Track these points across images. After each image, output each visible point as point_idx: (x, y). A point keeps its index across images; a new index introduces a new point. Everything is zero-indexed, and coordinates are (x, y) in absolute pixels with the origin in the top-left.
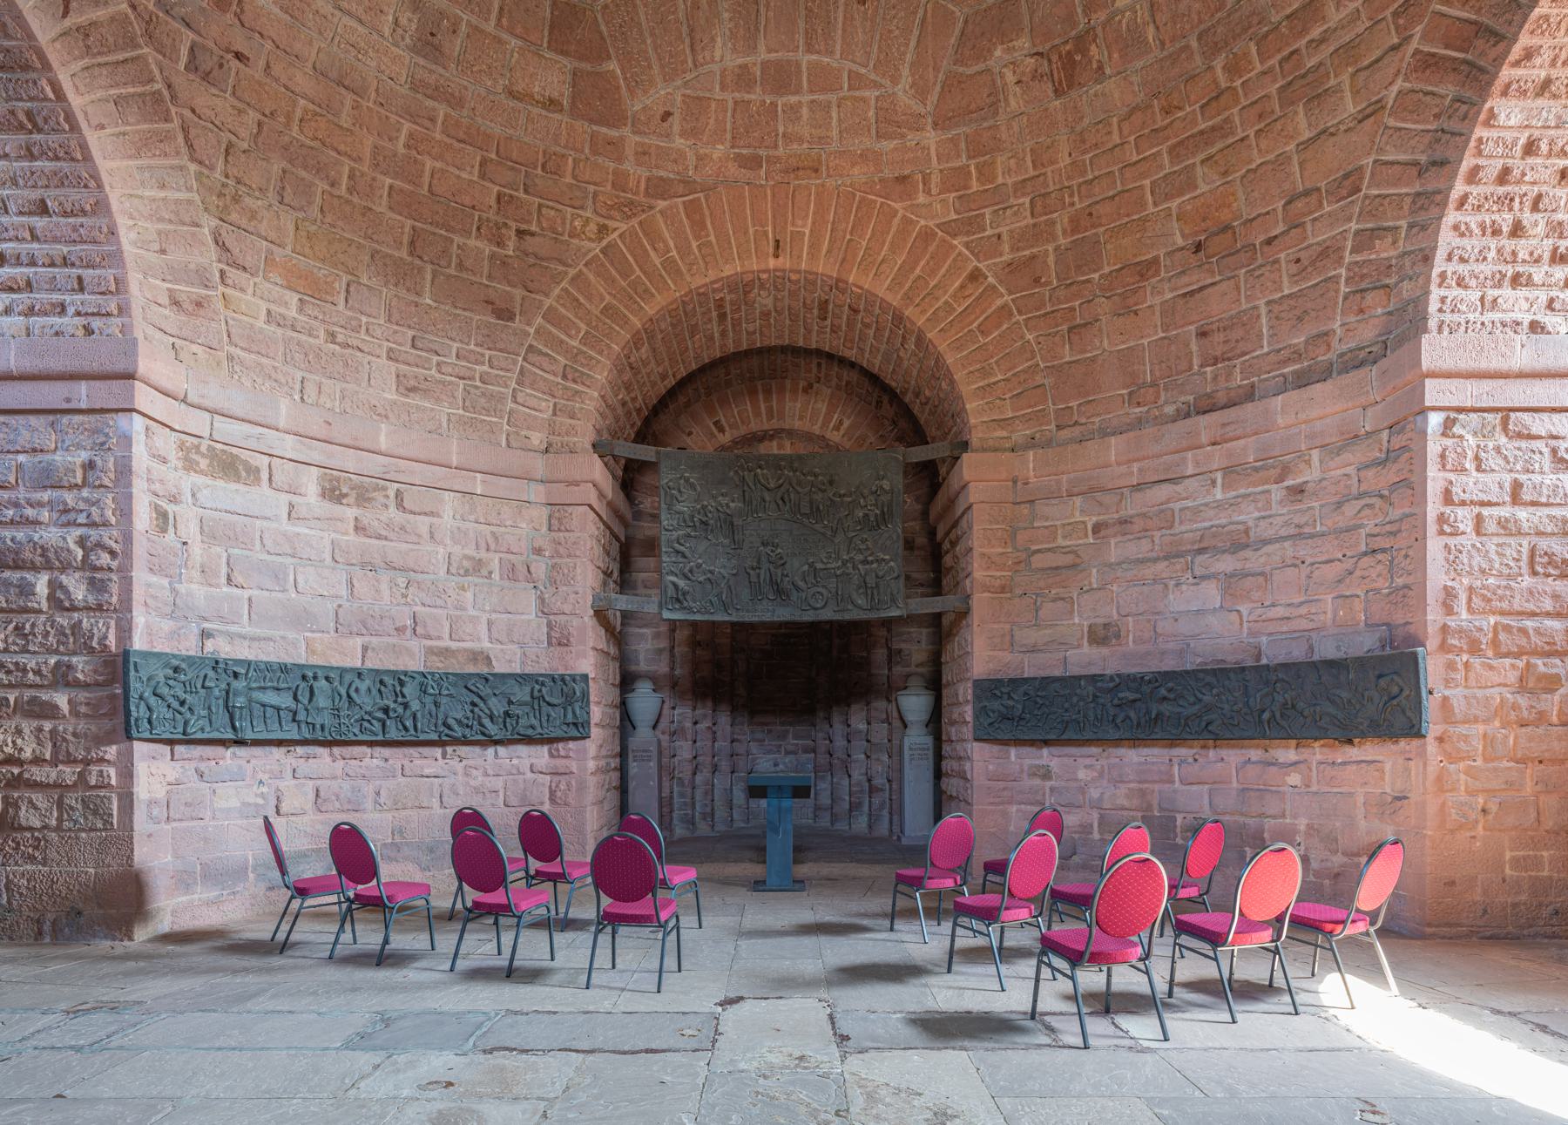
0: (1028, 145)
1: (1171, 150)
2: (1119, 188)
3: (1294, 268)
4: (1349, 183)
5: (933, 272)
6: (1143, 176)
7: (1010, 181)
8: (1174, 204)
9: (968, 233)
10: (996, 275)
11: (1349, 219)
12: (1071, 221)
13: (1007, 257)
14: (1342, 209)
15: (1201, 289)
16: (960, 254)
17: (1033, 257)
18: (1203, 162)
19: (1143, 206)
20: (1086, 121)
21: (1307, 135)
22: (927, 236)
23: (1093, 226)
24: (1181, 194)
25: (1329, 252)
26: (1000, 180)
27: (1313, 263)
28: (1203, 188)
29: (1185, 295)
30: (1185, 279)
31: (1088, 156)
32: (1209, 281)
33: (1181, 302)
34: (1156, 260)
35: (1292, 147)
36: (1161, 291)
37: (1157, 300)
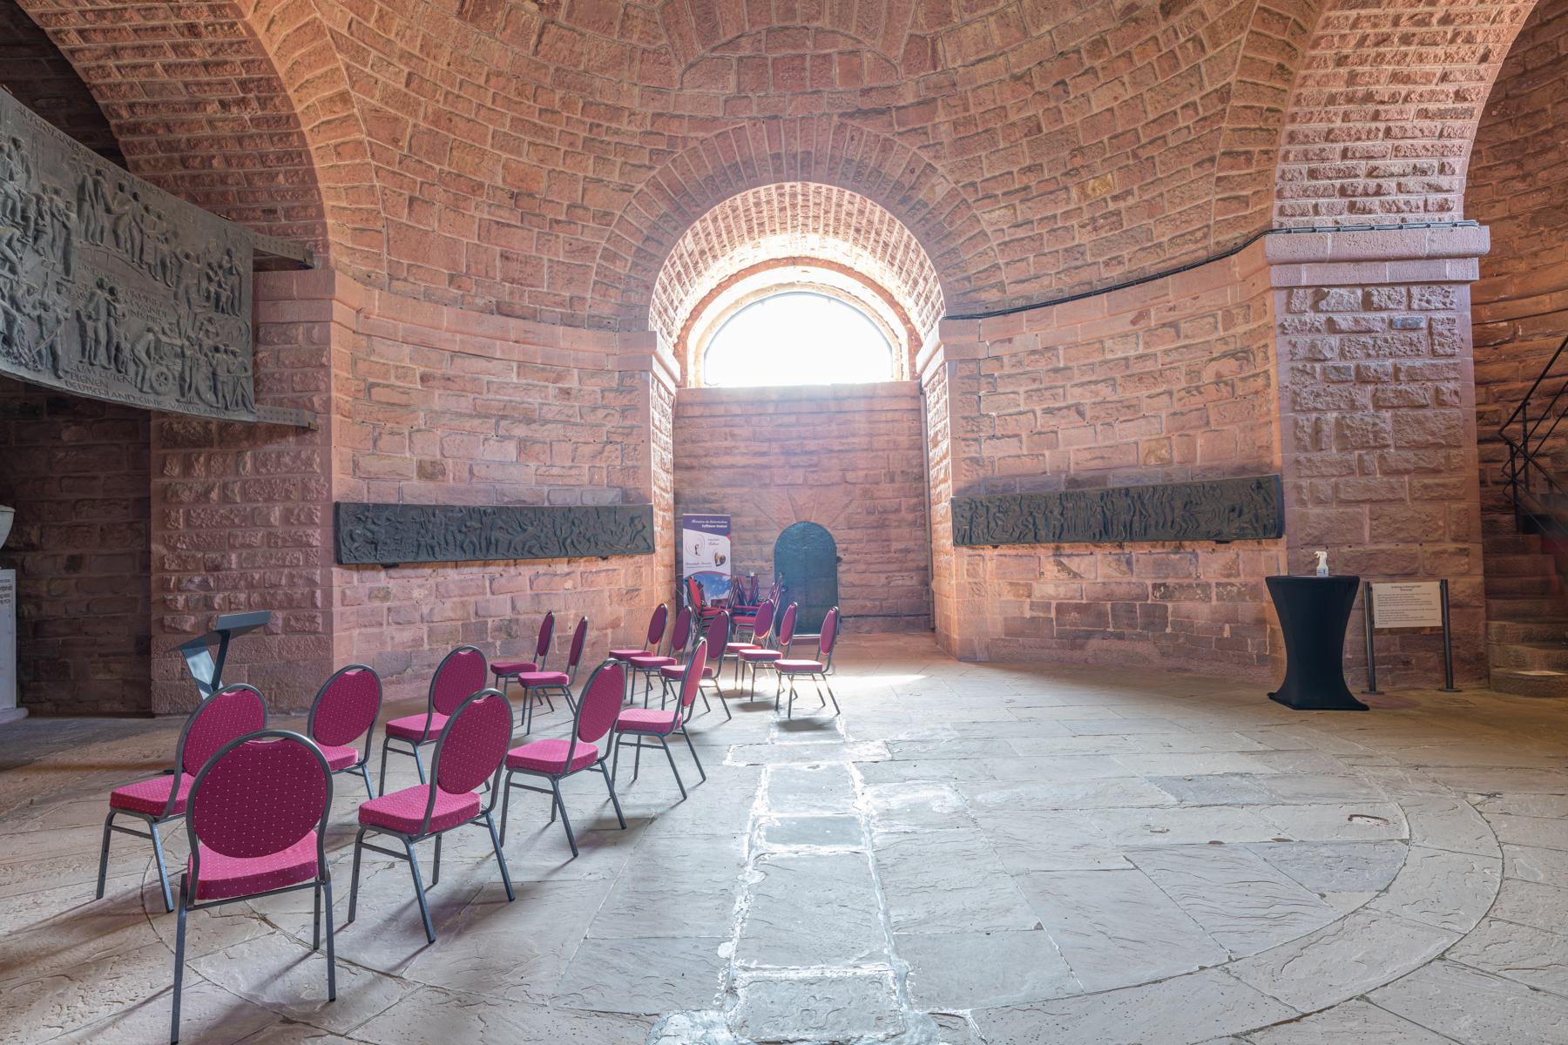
0: (423, 30)
1: (513, 119)
2: (473, 116)
3: (567, 247)
4: (605, 217)
5: (310, 67)
6: (491, 121)
7: (400, 45)
8: (505, 156)
9: (352, 58)
10: (362, 111)
11: (602, 238)
12: (434, 113)
13: (376, 102)
14: (600, 230)
15: (509, 225)
16: (338, 69)
17: (396, 119)
18: (530, 143)
19: (485, 142)
20: (468, 52)
21: (590, 174)
22: (316, 29)
23: (449, 130)
24: (511, 152)
25: (587, 249)
26: (392, 36)
27: (579, 251)
28: (524, 159)
29: (498, 223)
30: (501, 212)
31: (460, 77)
32: (514, 223)
33: (495, 226)
34: (481, 185)
35: (581, 175)
36: (479, 212)
37: (478, 215)
